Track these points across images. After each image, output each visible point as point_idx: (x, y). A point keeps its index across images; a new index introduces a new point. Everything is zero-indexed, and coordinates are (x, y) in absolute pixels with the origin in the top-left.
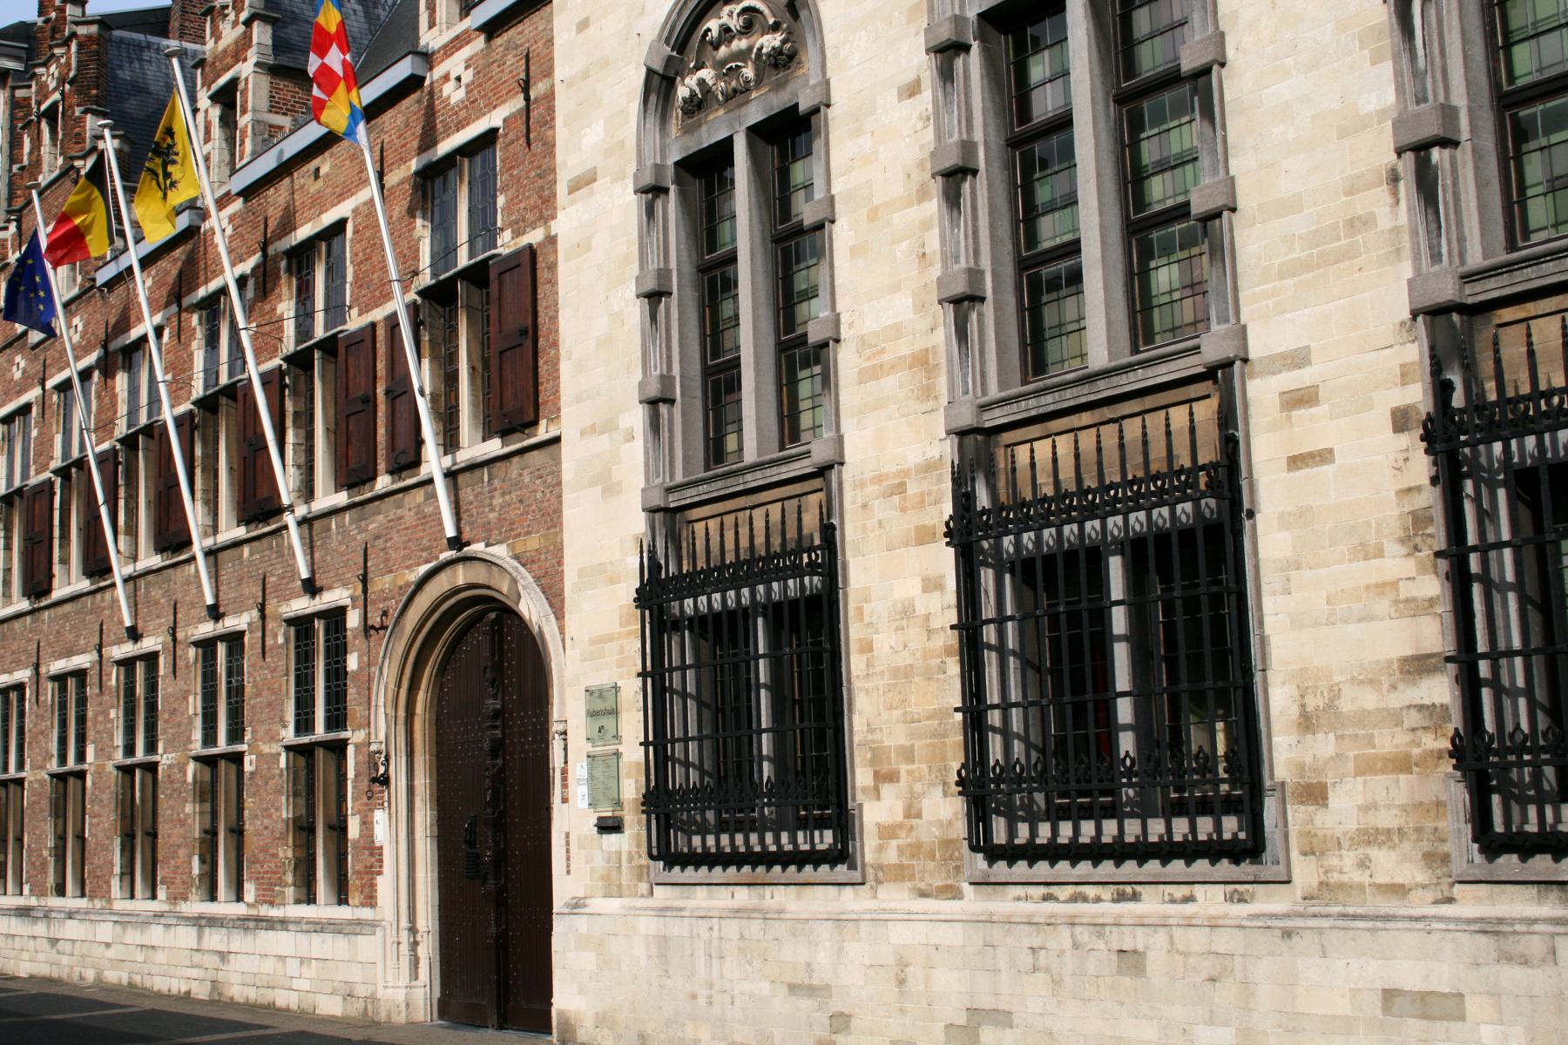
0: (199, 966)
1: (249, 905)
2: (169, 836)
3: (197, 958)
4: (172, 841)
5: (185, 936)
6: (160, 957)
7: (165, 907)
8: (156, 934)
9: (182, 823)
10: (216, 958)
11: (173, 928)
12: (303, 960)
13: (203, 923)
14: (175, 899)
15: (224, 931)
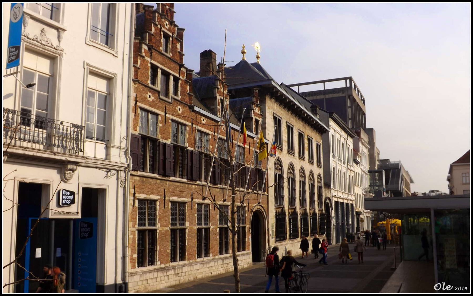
0: (223, 267)
1: (230, 254)
2: (213, 243)
3: (222, 266)
4: (213, 244)
5: (220, 262)
6: (214, 268)
7: (212, 258)
8: (213, 264)
9: (216, 241)
10: (227, 265)
11: (217, 262)
12: (242, 260)
13: (223, 259)
14: (214, 256)
15: (228, 259)
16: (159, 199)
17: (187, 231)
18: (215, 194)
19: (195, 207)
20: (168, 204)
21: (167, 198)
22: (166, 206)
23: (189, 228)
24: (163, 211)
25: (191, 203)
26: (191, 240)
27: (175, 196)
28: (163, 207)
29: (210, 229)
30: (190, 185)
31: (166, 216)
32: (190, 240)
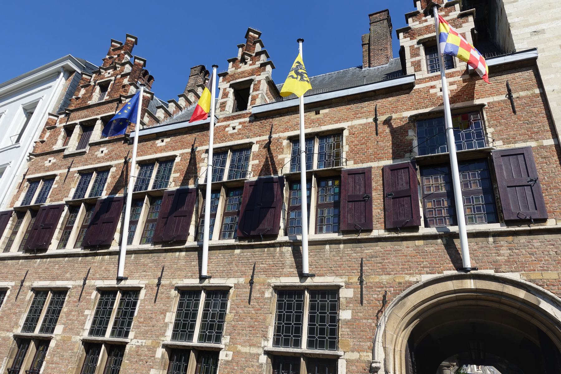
16: (12, 287)
17: (52, 344)
18: (167, 264)
19: (91, 296)
20: (25, 293)
21: (26, 284)
22: (19, 297)
23: (58, 338)
24: (12, 305)
25: (80, 289)
26: (58, 364)
27: (45, 279)
28: (15, 299)
29: (128, 347)
30: (89, 258)
31: (15, 313)
32: (53, 364)
